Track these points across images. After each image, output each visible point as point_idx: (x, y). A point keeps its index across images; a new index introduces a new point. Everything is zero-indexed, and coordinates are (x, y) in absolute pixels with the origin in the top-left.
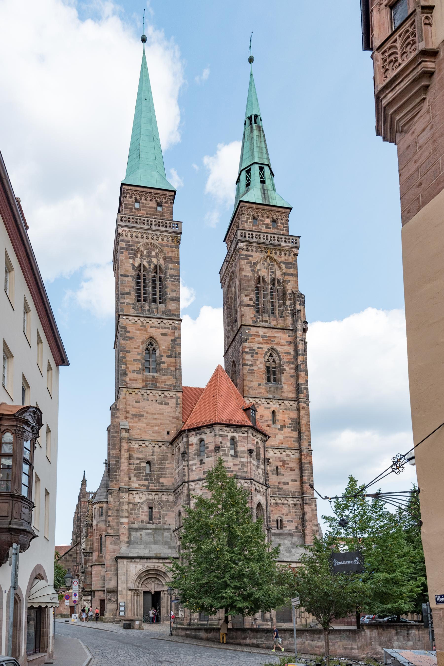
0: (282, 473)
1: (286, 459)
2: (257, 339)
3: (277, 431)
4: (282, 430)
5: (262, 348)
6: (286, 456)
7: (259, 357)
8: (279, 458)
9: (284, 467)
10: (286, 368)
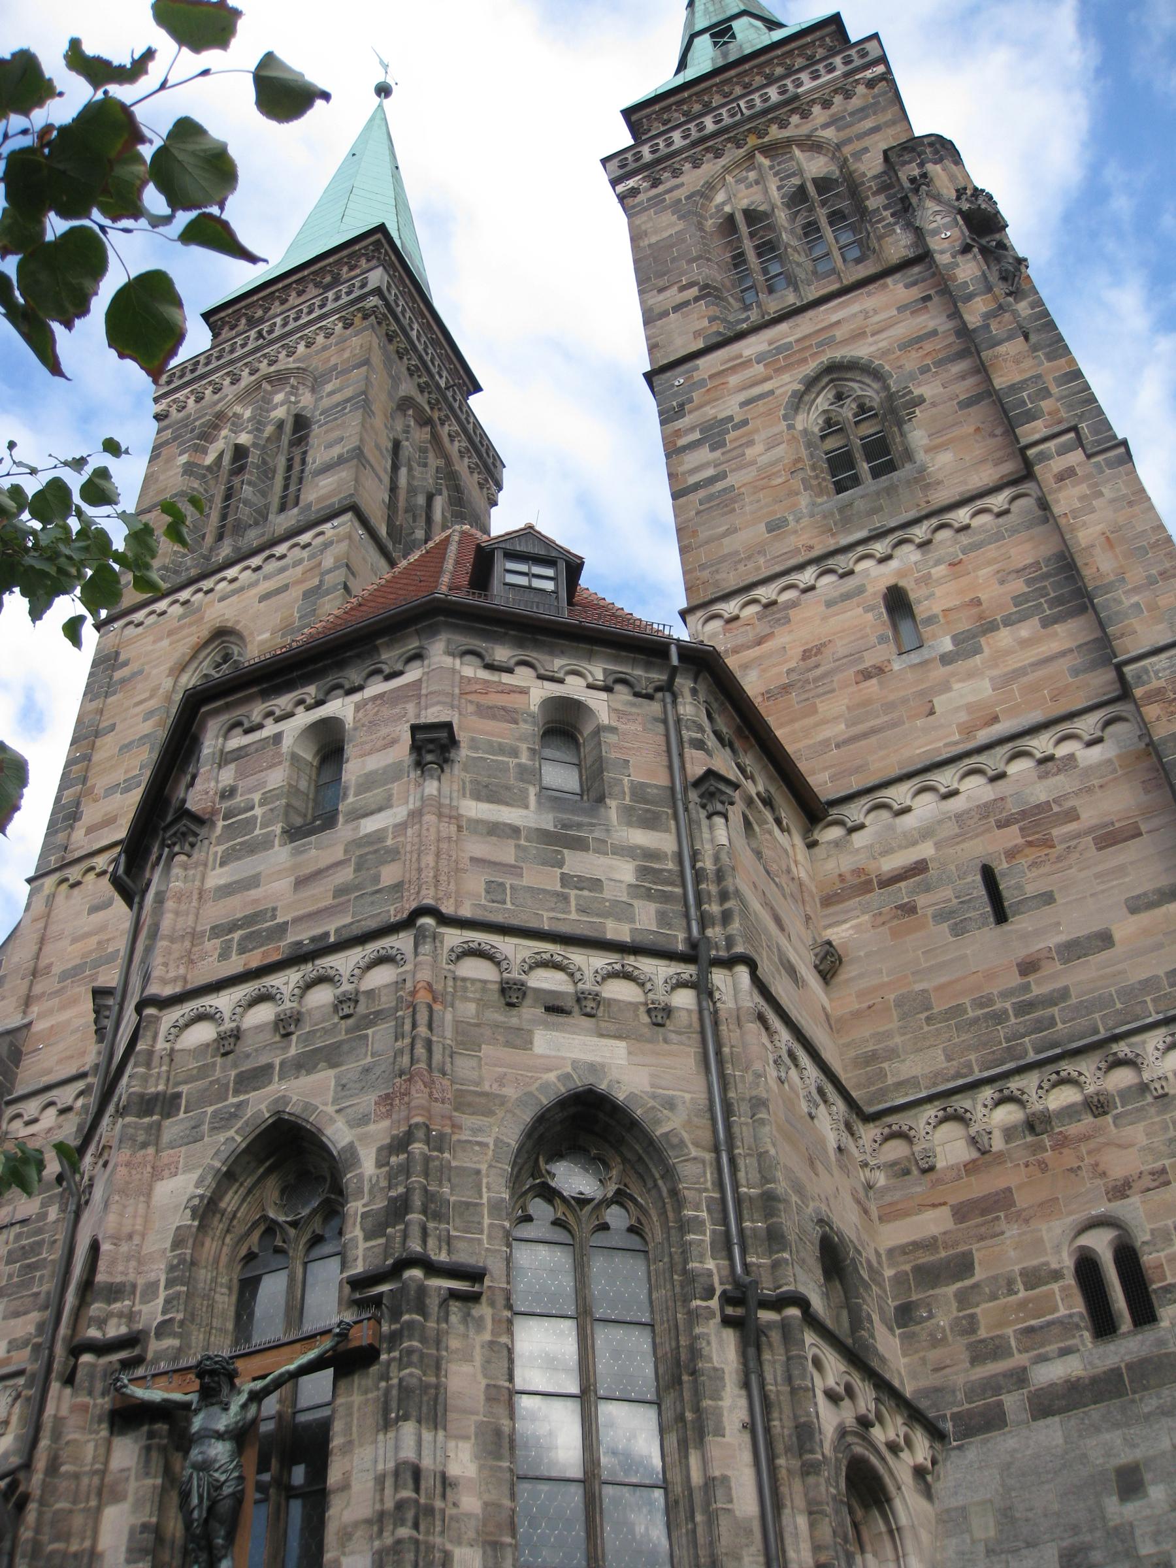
0: (1031, 890)
1: (1041, 792)
2: (734, 380)
3: (942, 671)
4: (977, 651)
5: (772, 392)
6: (1042, 777)
7: (757, 431)
8: (986, 810)
9: (1048, 843)
10: (927, 389)
